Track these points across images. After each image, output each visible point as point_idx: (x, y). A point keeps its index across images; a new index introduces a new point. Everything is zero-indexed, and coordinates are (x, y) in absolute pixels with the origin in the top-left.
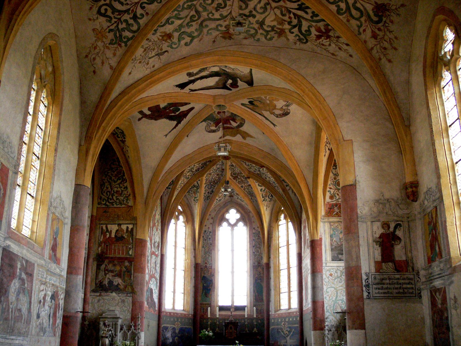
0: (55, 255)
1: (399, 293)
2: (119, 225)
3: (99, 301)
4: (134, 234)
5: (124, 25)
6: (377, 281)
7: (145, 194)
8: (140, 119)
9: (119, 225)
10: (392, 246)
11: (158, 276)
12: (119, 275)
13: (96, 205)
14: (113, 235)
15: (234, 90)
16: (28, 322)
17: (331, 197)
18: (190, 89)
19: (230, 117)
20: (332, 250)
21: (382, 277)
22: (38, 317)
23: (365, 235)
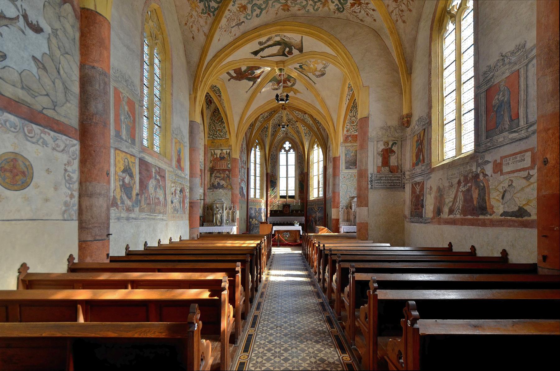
0: (180, 165)
1: (391, 185)
2: (222, 150)
3: (212, 194)
4: (231, 155)
6: (377, 178)
7: (236, 131)
8: (229, 80)
9: (222, 150)
10: (389, 156)
11: (246, 180)
12: (223, 179)
13: (207, 139)
14: (218, 156)
15: (290, 56)
16: (165, 205)
17: (347, 131)
18: (261, 56)
19: (287, 78)
20: (346, 162)
21: (381, 176)
22: (172, 202)
23: (372, 150)
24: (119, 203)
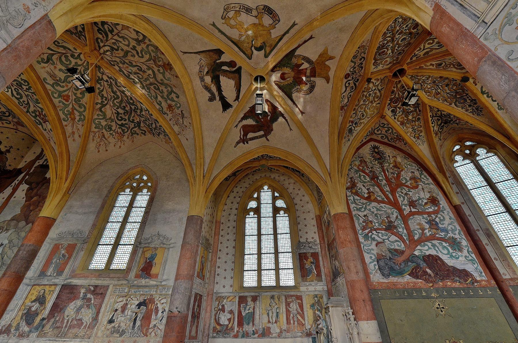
24: (12, 330)
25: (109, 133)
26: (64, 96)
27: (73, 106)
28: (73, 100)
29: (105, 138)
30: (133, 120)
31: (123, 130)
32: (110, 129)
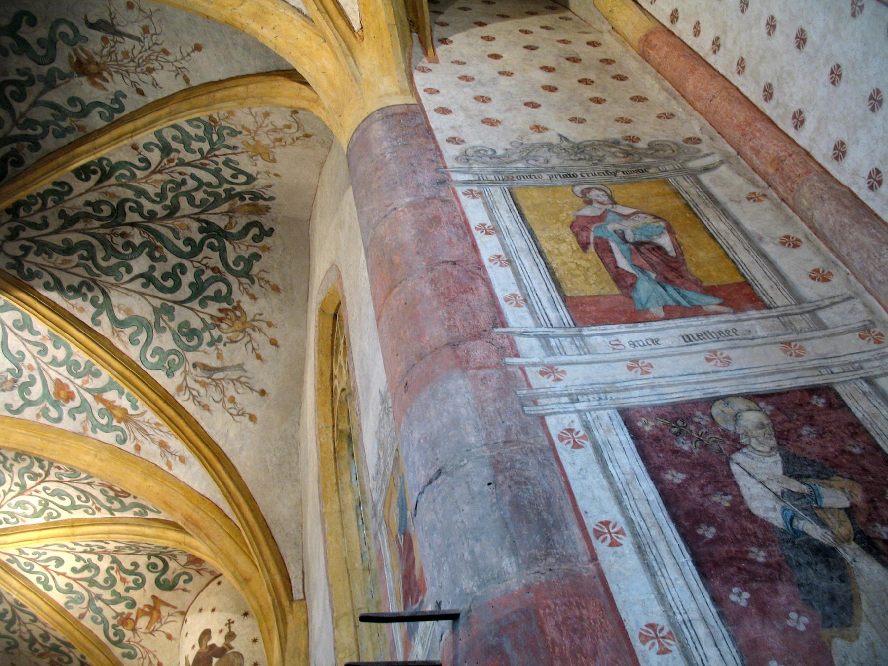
5: (195, 145)
25: (204, 347)
26: (57, 394)
27: (88, 390)
28: (72, 378)
29: (216, 370)
30: (189, 241)
31: (217, 297)
32: (193, 333)
